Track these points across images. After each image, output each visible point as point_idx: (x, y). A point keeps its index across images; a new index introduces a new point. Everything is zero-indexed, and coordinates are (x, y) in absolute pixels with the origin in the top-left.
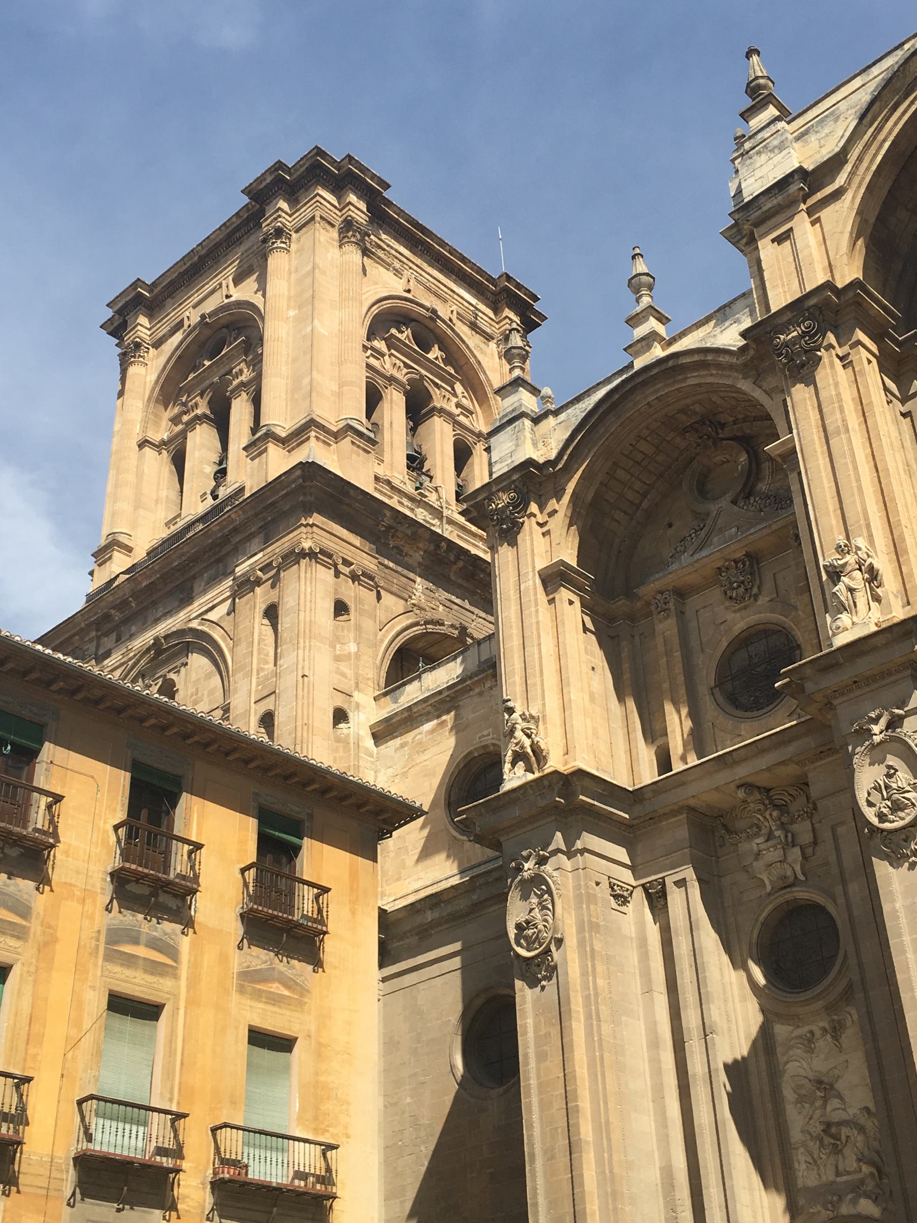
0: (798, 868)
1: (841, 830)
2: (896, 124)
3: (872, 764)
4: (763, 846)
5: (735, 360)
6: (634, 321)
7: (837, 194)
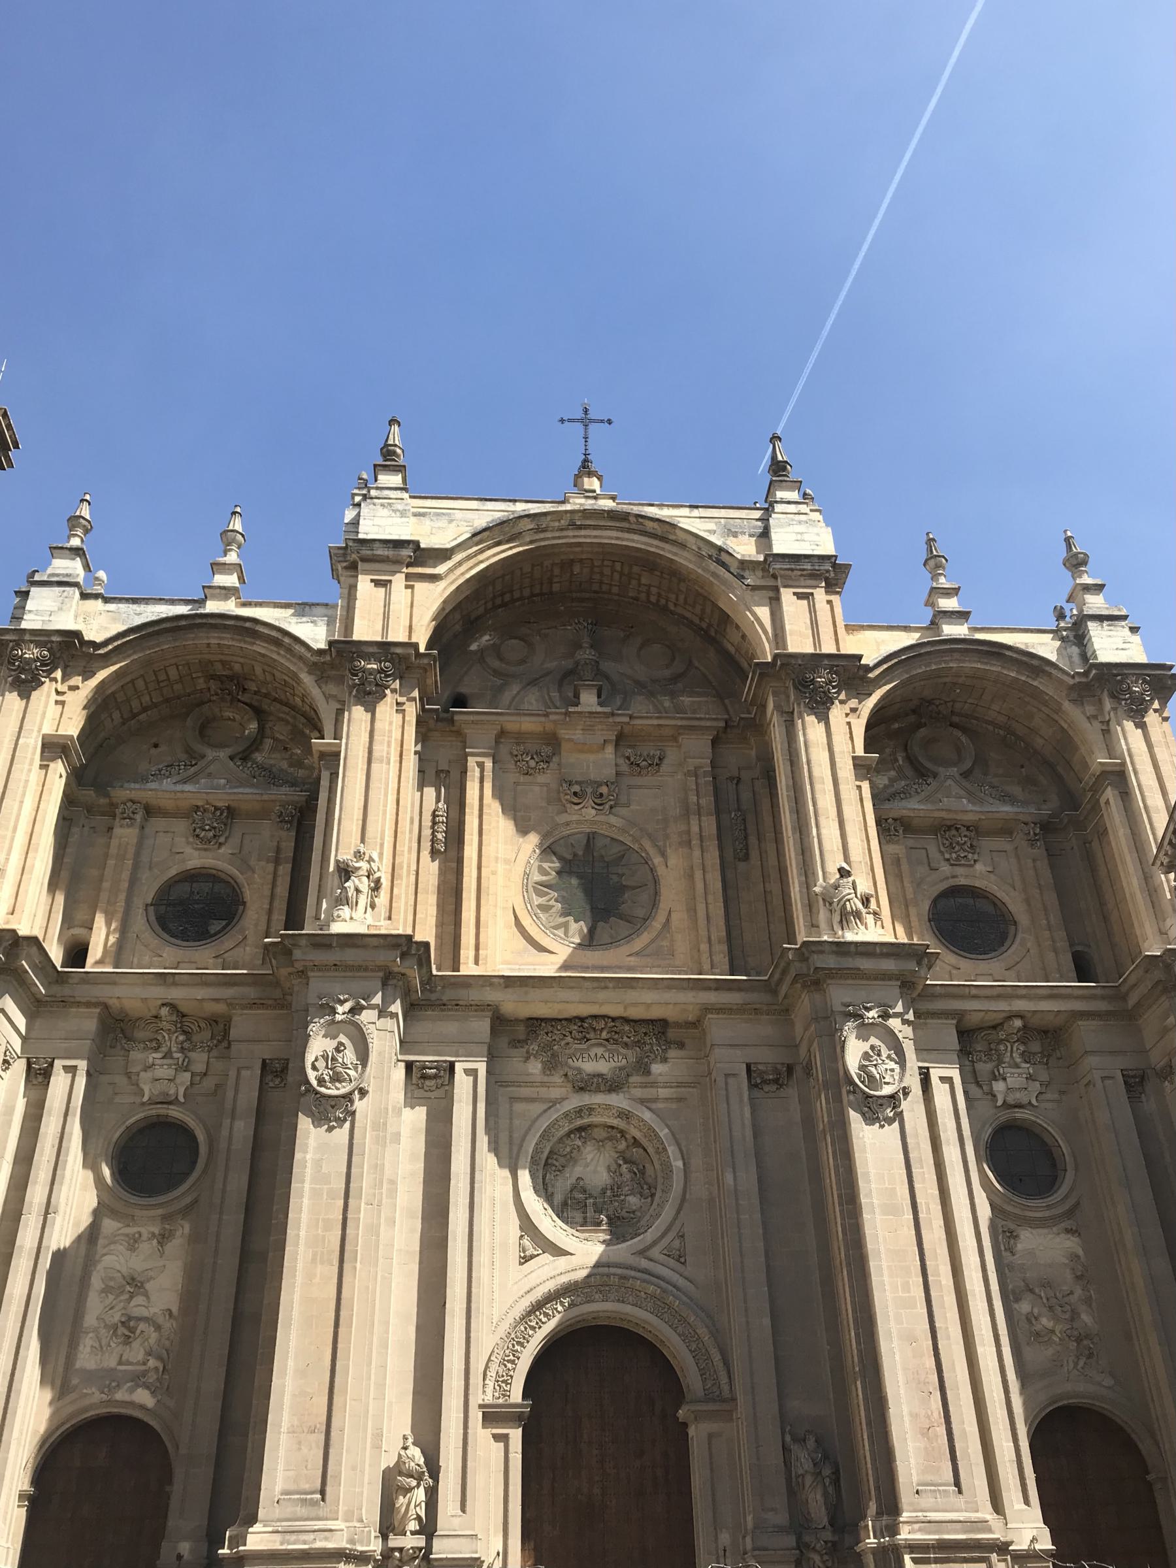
0: (181, 1091)
1: (244, 1073)
2: (494, 555)
3: (325, 1036)
4: (158, 1062)
5: (309, 655)
6: (218, 567)
7: (434, 578)
